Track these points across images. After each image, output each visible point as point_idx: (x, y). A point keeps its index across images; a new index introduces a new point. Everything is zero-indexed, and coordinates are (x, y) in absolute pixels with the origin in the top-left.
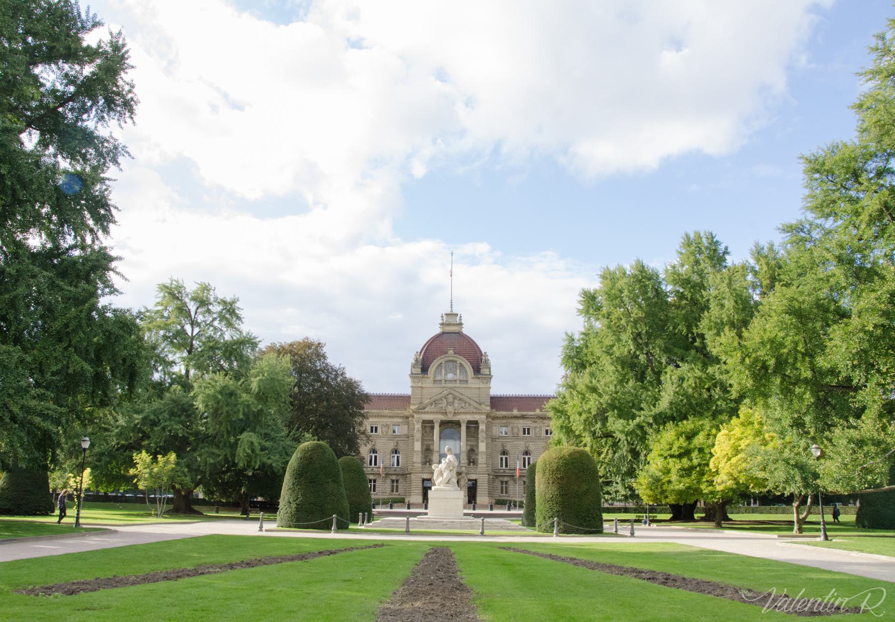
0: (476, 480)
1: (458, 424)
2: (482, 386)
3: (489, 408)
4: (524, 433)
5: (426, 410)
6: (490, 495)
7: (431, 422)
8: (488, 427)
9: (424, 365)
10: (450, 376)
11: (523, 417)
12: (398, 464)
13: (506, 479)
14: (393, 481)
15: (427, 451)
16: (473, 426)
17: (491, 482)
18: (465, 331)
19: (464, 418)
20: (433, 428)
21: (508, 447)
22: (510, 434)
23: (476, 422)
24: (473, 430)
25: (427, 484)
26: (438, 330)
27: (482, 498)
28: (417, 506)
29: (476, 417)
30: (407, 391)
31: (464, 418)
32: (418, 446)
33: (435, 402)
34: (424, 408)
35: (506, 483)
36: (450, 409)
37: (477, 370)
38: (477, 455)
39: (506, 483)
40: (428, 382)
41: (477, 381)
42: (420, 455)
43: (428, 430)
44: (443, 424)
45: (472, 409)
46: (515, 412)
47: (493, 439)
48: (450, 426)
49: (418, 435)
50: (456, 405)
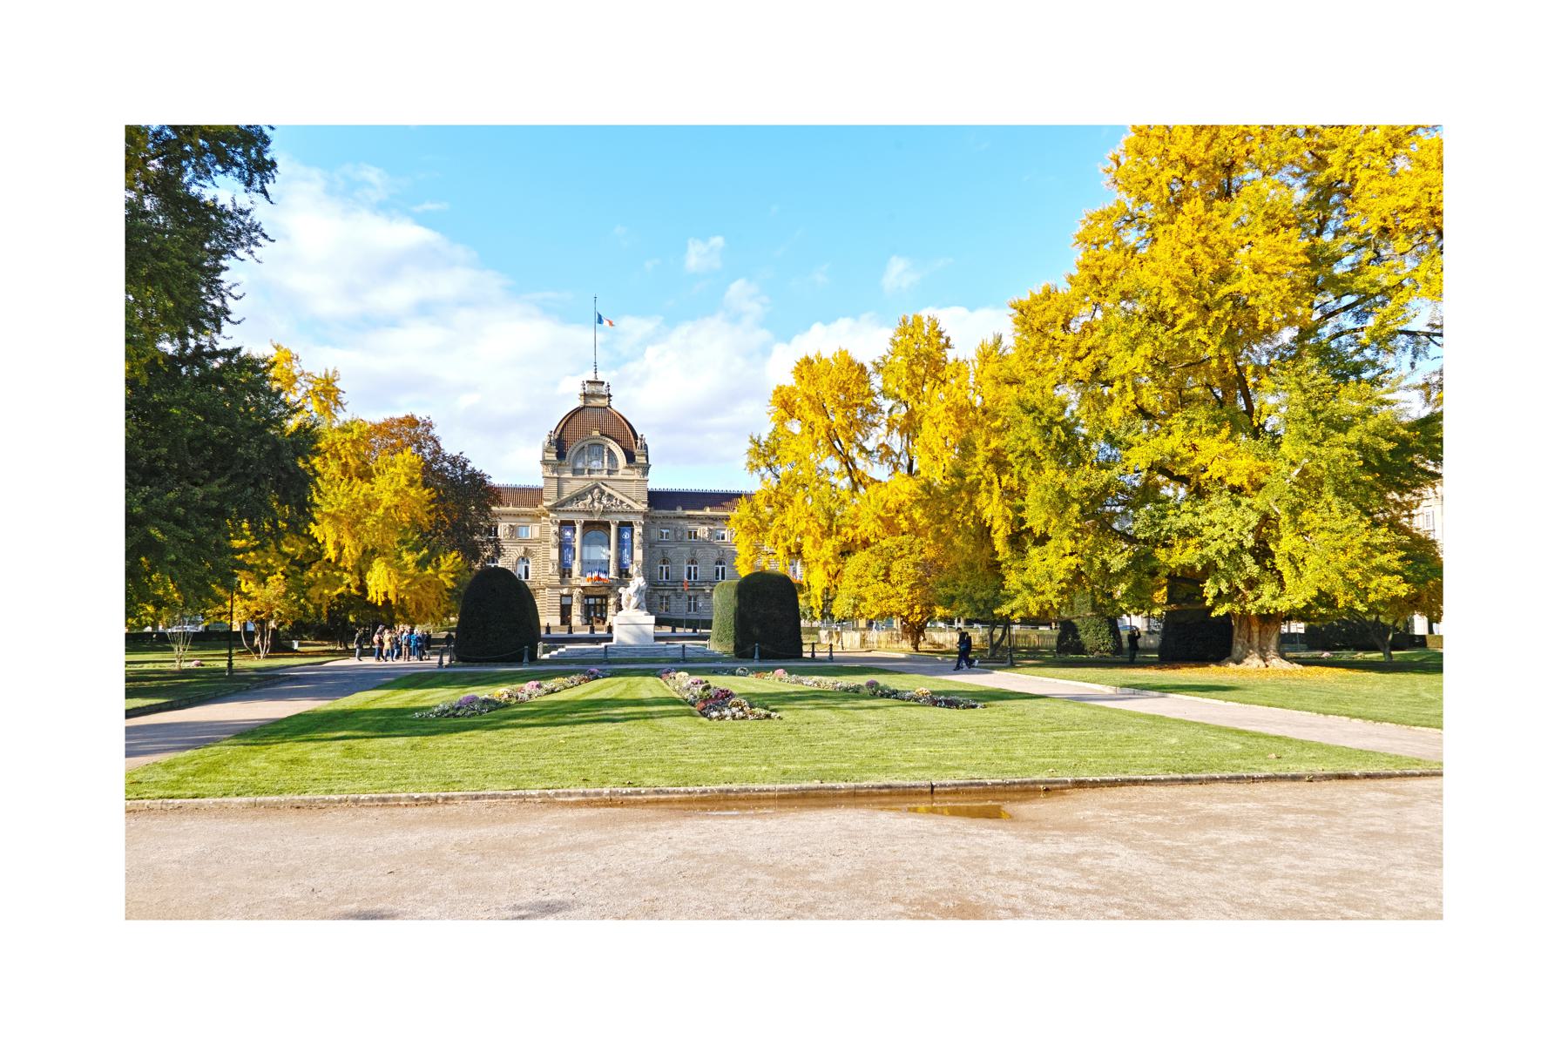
9: (560, 447)
16: (625, 526)
18: (616, 405)
21: (670, 554)
22: (671, 538)
23: (630, 524)
25: (566, 601)
29: (631, 518)
30: (540, 483)
37: (630, 458)
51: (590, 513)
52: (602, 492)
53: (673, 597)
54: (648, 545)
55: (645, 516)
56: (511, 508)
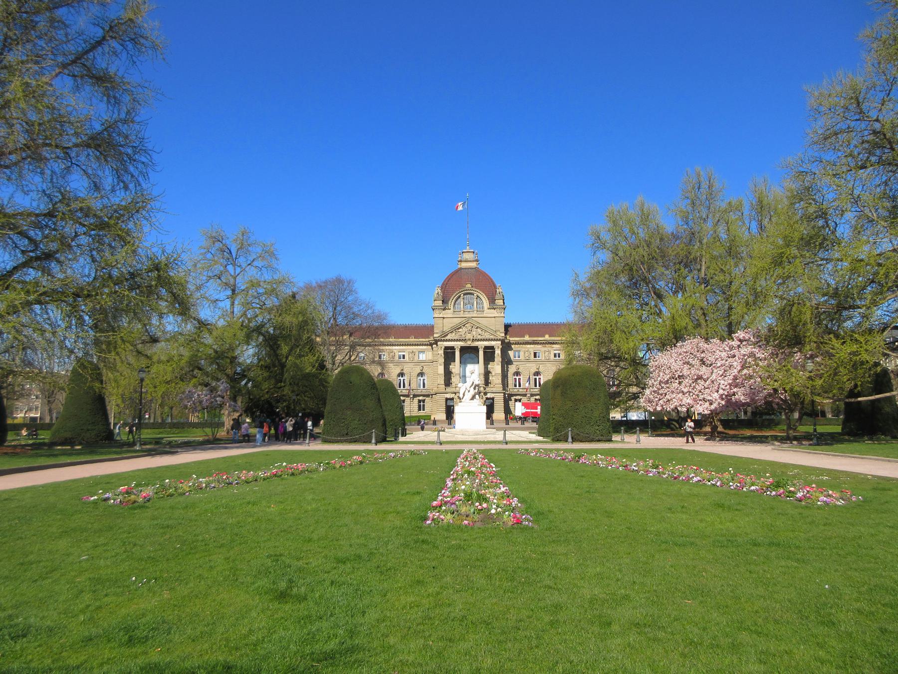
0: (493, 399)
1: (476, 349)
5: (448, 337)
7: (453, 348)
11: (534, 343)
12: (424, 386)
14: (420, 401)
15: (448, 374)
19: (481, 344)
23: (492, 348)
25: (450, 403)
27: (499, 415)
29: (493, 343)
31: (481, 344)
33: (456, 328)
44: (463, 350)
45: (487, 336)
46: (527, 338)
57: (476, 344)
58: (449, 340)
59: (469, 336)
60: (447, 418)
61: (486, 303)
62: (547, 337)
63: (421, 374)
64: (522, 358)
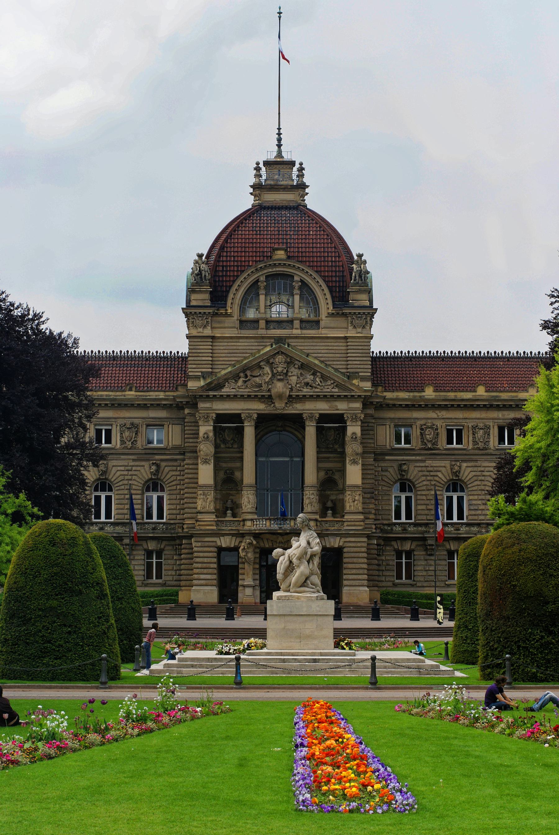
1: (298, 421)
2: (351, 333)
3: (367, 385)
4: (450, 442)
5: (226, 390)
6: (373, 582)
7: (236, 418)
8: (367, 429)
10: (279, 311)
13: (407, 546)
15: (227, 483)
17: (374, 556)
18: (313, 202)
20: (240, 432)
21: (413, 473)
23: (340, 418)
24: (332, 435)
25: (228, 560)
26: (246, 202)
28: (209, 610)
29: (341, 407)
32: (206, 474)
33: (245, 371)
34: (220, 386)
35: (409, 554)
36: (279, 387)
37: (340, 298)
38: (343, 491)
39: (409, 554)
40: (227, 329)
41: (341, 322)
42: (211, 496)
43: (228, 436)
44: (264, 422)
45: (329, 389)
46: (429, 393)
47: (379, 455)
48: (279, 427)
49: (206, 449)
50: (294, 379)
51: (269, 399)
52: (290, 362)
53: (419, 553)
54: (374, 455)
55: (366, 402)
56: (131, 394)
57: (297, 408)
58: (229, 398)
59: (279, 387)
60: (222, 598)
61: (325, 304)
62: (481, 391)
63: (154, 484)
64: (416, 443)
